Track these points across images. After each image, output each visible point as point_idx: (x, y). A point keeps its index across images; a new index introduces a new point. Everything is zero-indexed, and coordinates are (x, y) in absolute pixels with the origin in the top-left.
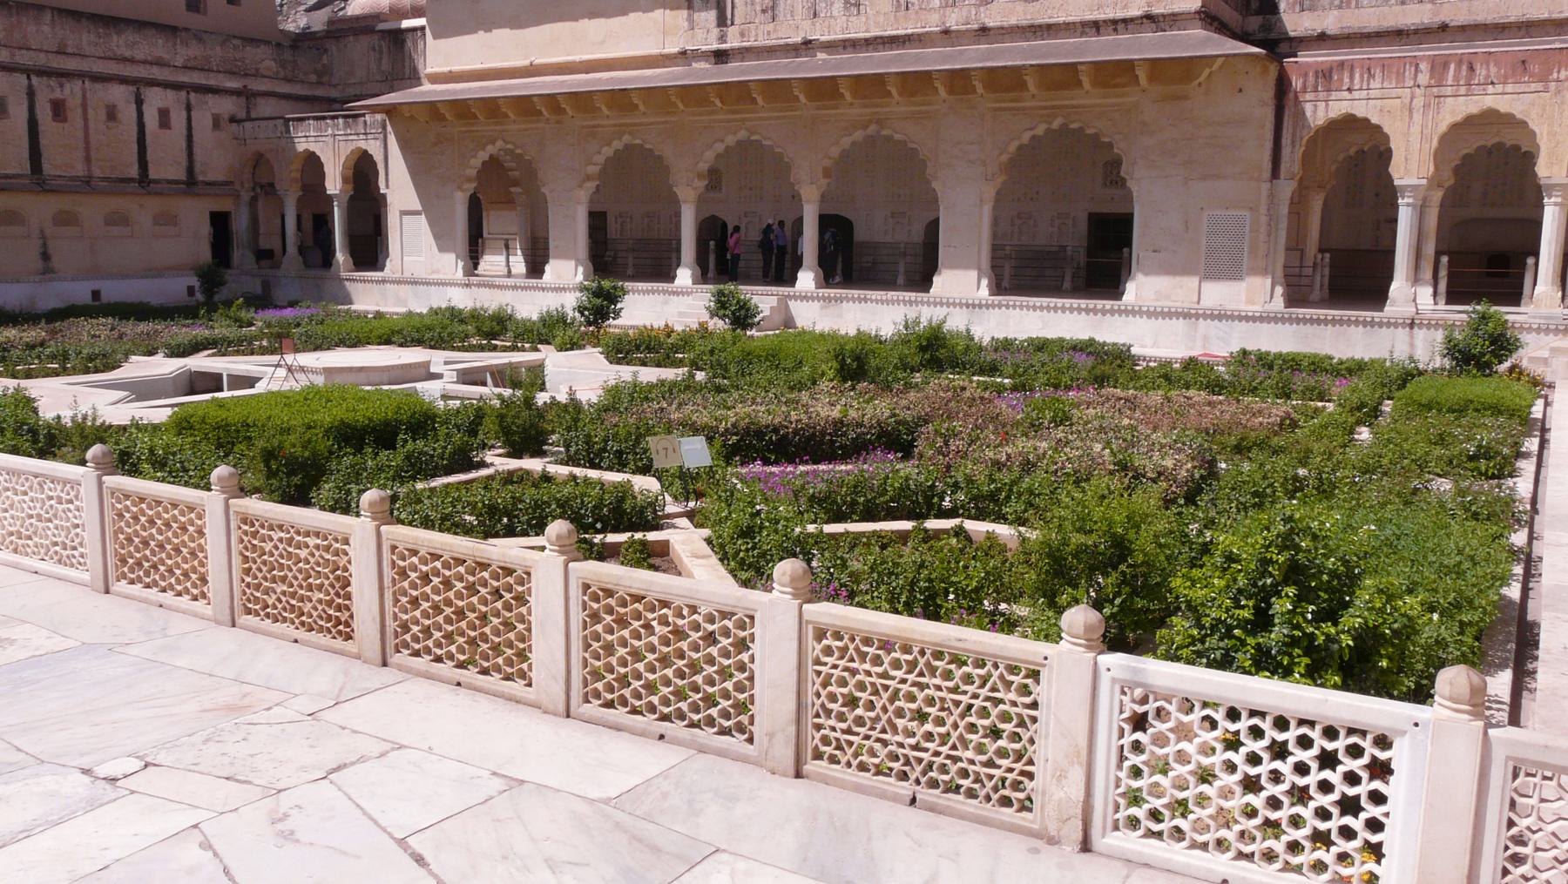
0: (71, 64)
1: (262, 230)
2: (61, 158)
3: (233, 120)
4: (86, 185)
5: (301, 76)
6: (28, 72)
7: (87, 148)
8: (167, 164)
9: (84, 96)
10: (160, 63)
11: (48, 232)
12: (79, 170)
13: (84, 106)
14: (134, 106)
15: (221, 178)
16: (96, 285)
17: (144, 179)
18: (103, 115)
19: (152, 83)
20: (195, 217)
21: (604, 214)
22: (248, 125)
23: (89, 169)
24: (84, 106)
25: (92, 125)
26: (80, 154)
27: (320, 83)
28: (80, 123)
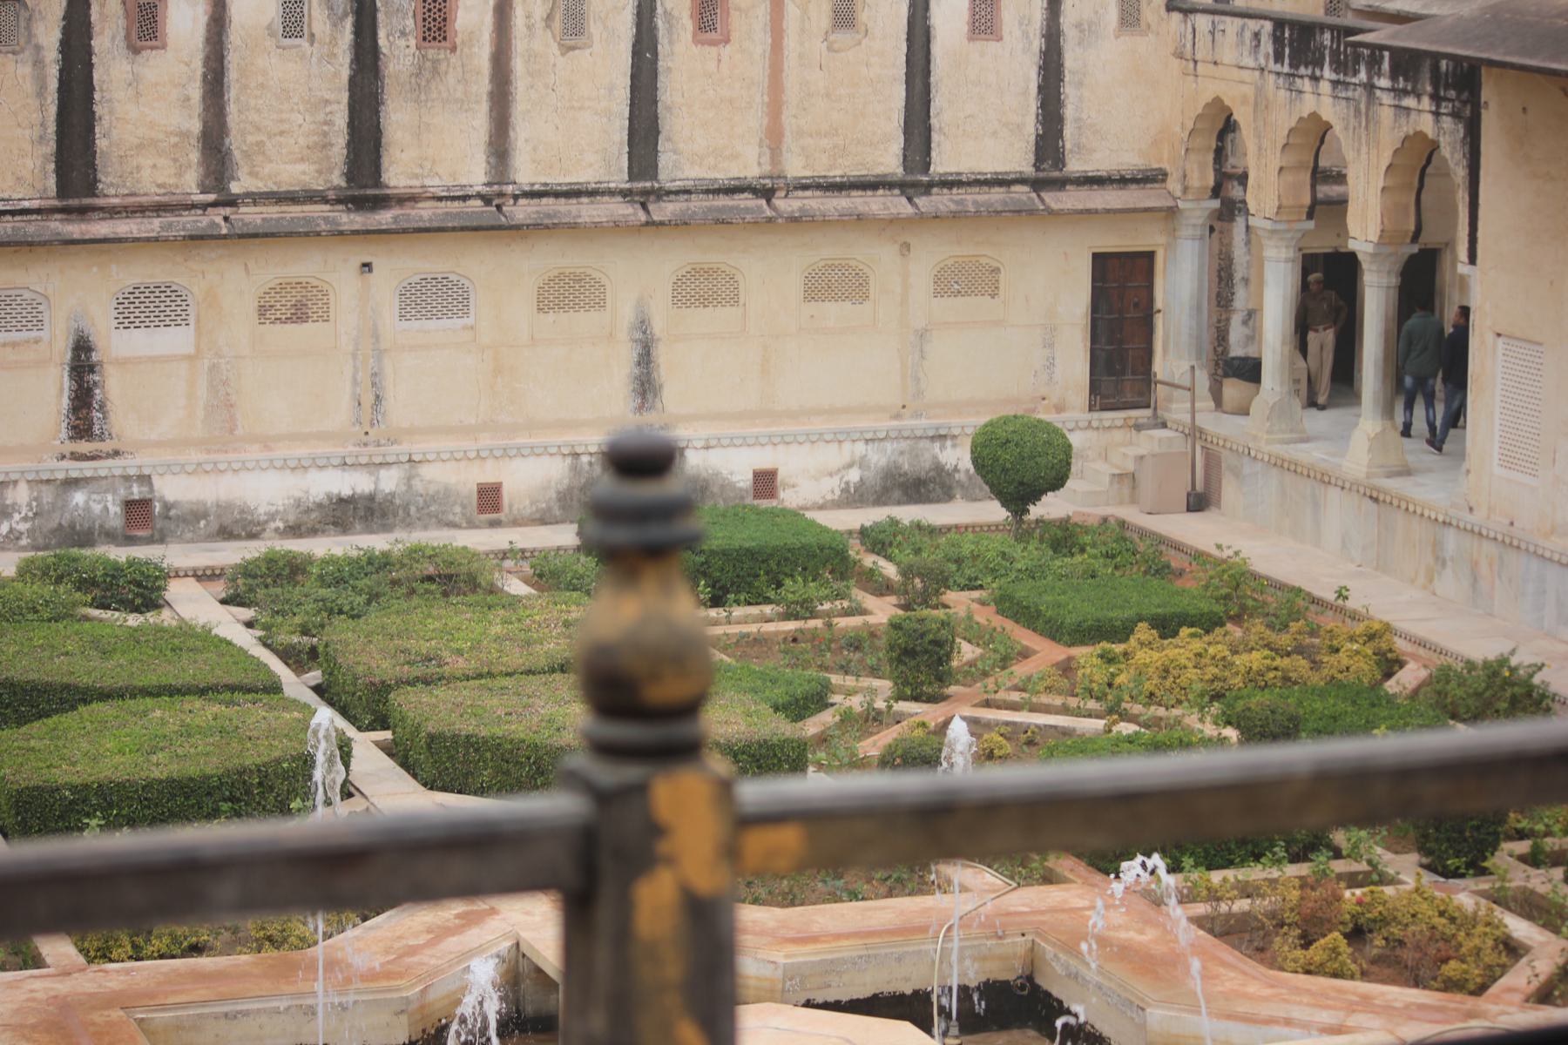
7: (775, 108)
11: (658, 327)
12: (750, 167)
16: (763, 459)
17: (917, 176)
25: (791, 43)
26: (755, 120)
28: (760, 43)
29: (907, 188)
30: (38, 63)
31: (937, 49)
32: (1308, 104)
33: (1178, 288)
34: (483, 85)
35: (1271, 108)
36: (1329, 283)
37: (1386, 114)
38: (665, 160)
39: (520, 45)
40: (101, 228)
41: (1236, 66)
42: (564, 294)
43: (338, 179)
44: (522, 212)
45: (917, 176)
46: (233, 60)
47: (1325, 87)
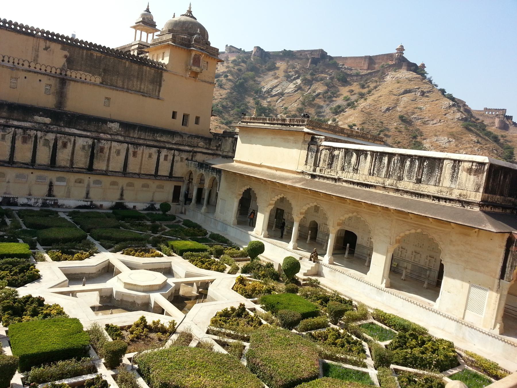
0: (141, 142)
3: (187, 159)
4: (139, 175)
5: (211, 148)
6: (128, 143)
8: (164, 171)
10: (168, 143)
12: (137, 171)
13: (143, 153)
15: (180, 176)
18: (147, 156)
19: (164, 148)
20: (169, 187)
24: (143, 153)
25: (144, 159)
26: (138, 166)
27: (217, 150)
28: (140, 158)
30: (50, 148)
32: (201, 172)
33: (183, 190)
34: (107, 158)
36: (200, 191)
38: (127, 170)
39: (112, 154)
40: (56, 169)
41: (192, 167)
42: (113, 183)
43: (87, 167)
46: (75, 151)
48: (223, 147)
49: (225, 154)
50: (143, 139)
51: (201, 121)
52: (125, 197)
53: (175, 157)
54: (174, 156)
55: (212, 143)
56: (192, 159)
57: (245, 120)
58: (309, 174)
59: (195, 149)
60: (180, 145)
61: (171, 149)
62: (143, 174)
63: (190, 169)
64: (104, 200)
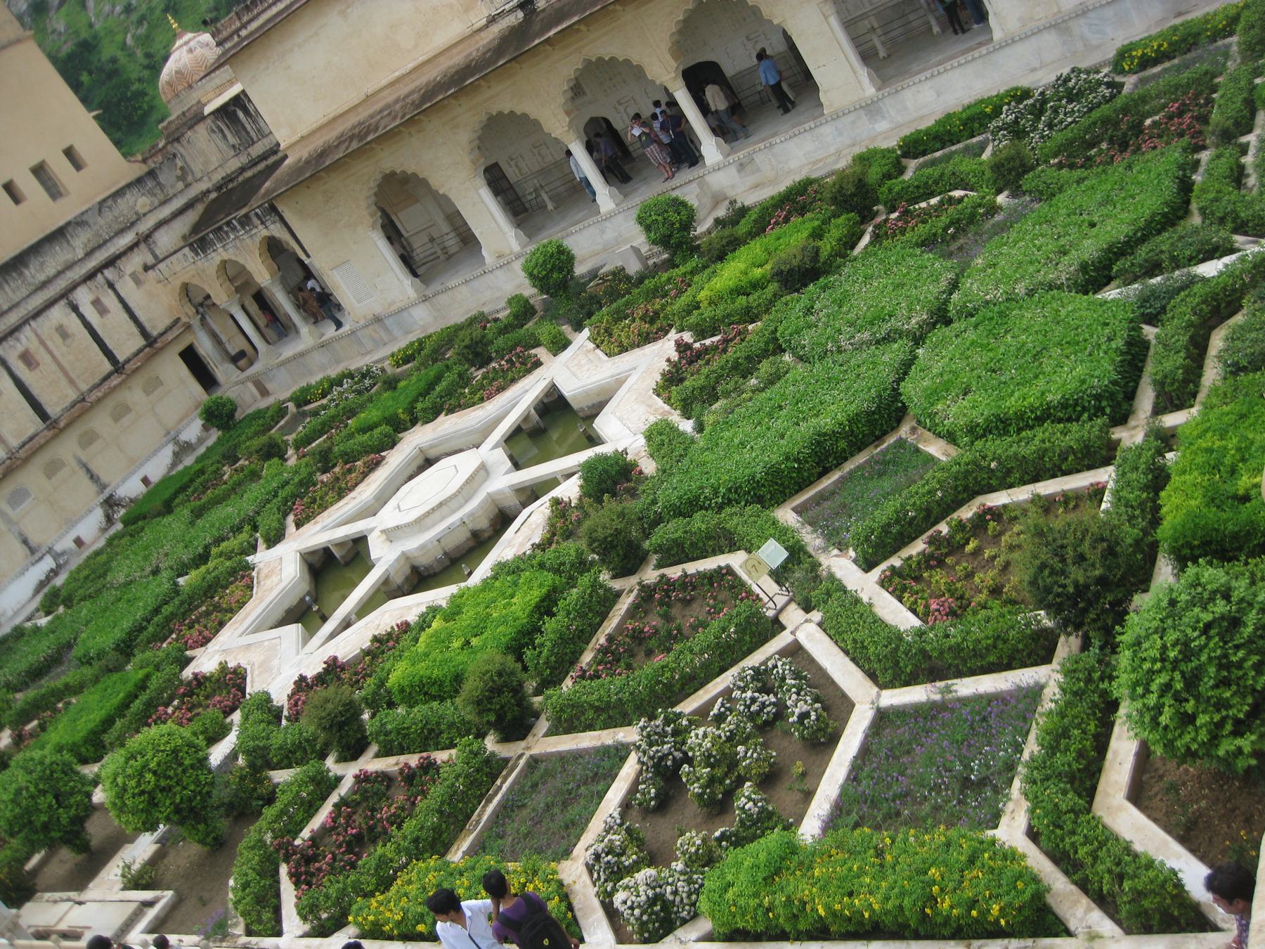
0: (13, 319)
1: (224, 338)
2: (56, 399)
3: (147, 268)
5: (171, 192)
7: (66, 374)
8: (126, 343)
9: (37, 335)
10: (69, 266)
11: (84, 459)
12: (72, 395)
13: (42, 343)
14: (74, 315)
16: (140, 475)
17: (118, 367)
19: (74, 287)
20: (173, 369)
21: (496, 164)
22: (162, 266)
23: (78, 389)
24: (42, 343)
26: (64, 382)
27: (188, 186)
29: (116, 371)
31: (95, 327)
33: (205, 348)
35: (203, 271)
37: (248, 241)
38: (49, 410)
42: (52, 469)
44: (22, 454)
45: (118, 367)
47: (220, 250)
48: (197, 167)
49: (217, 177)
50: (10, 309)
51: (82, 151)
52: (104, 478)
53: (118, 287)
54: (111, 286)
55: (162, 178)
56: (155, 256)
57: (225, 34)
58: (511, 11)
59: (144, 226)
60: (100, 247)
61: (91, 276)
62: (91, 390)
63: (177, 283)
64: (71, 523)
